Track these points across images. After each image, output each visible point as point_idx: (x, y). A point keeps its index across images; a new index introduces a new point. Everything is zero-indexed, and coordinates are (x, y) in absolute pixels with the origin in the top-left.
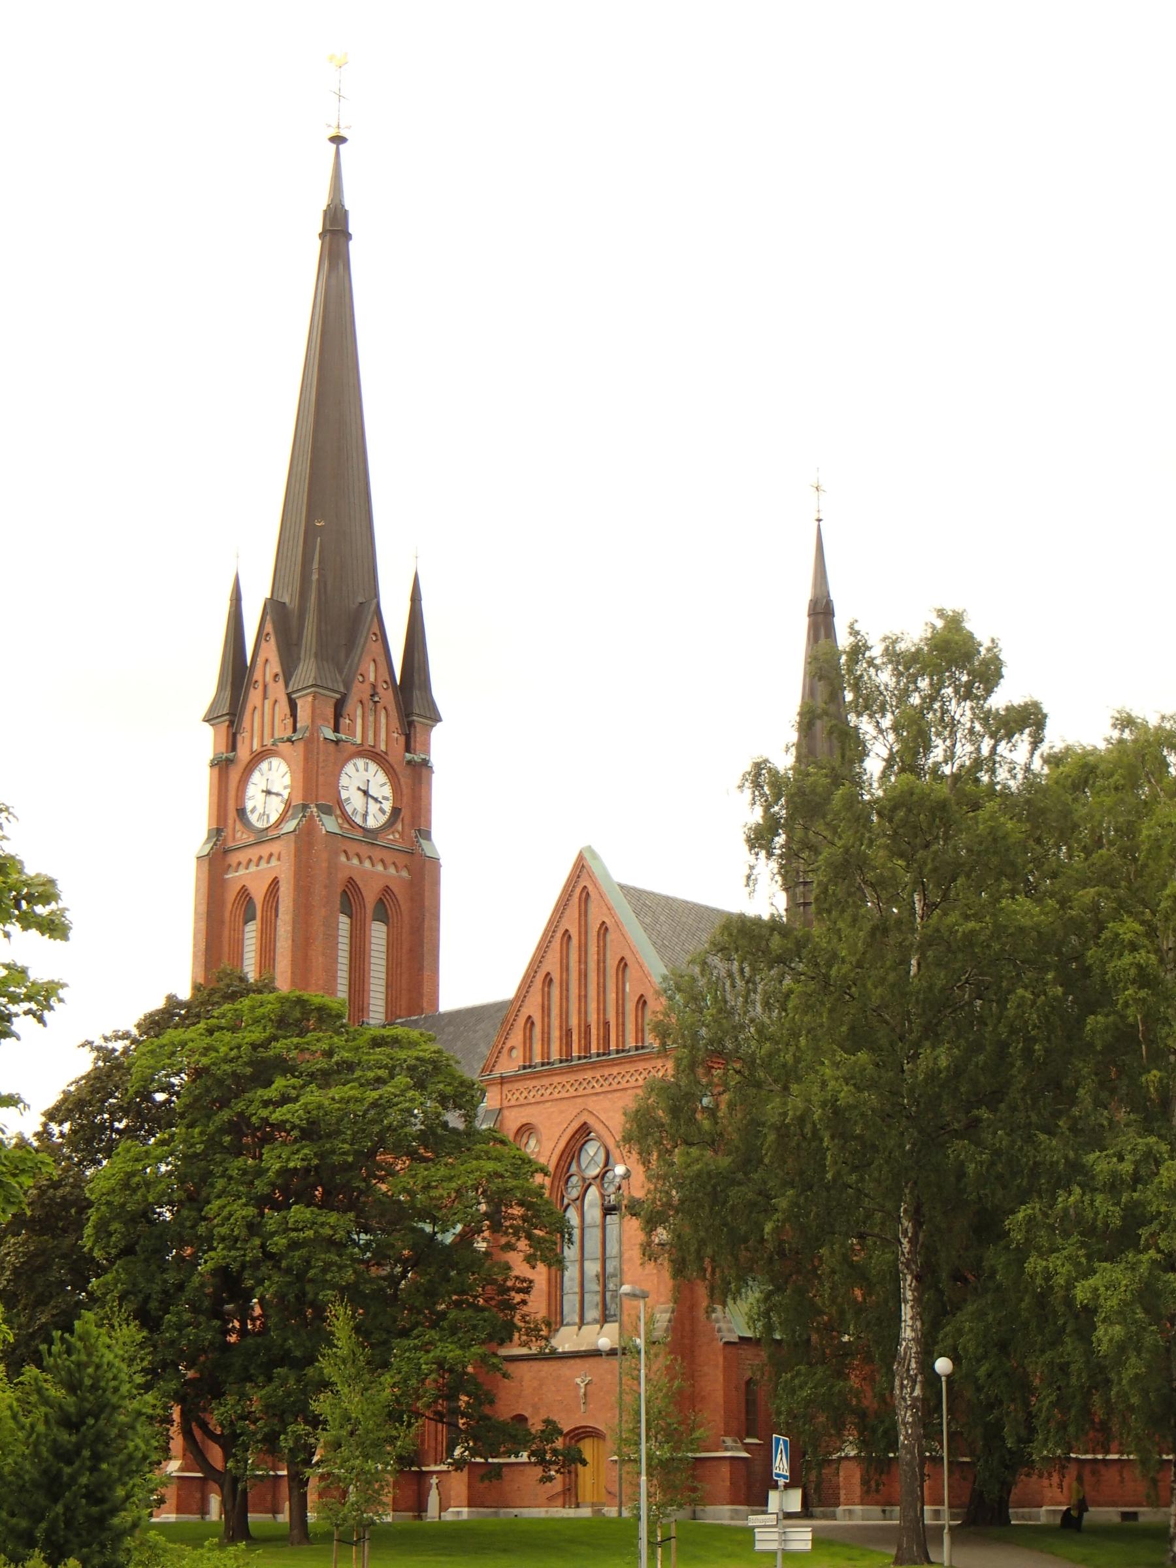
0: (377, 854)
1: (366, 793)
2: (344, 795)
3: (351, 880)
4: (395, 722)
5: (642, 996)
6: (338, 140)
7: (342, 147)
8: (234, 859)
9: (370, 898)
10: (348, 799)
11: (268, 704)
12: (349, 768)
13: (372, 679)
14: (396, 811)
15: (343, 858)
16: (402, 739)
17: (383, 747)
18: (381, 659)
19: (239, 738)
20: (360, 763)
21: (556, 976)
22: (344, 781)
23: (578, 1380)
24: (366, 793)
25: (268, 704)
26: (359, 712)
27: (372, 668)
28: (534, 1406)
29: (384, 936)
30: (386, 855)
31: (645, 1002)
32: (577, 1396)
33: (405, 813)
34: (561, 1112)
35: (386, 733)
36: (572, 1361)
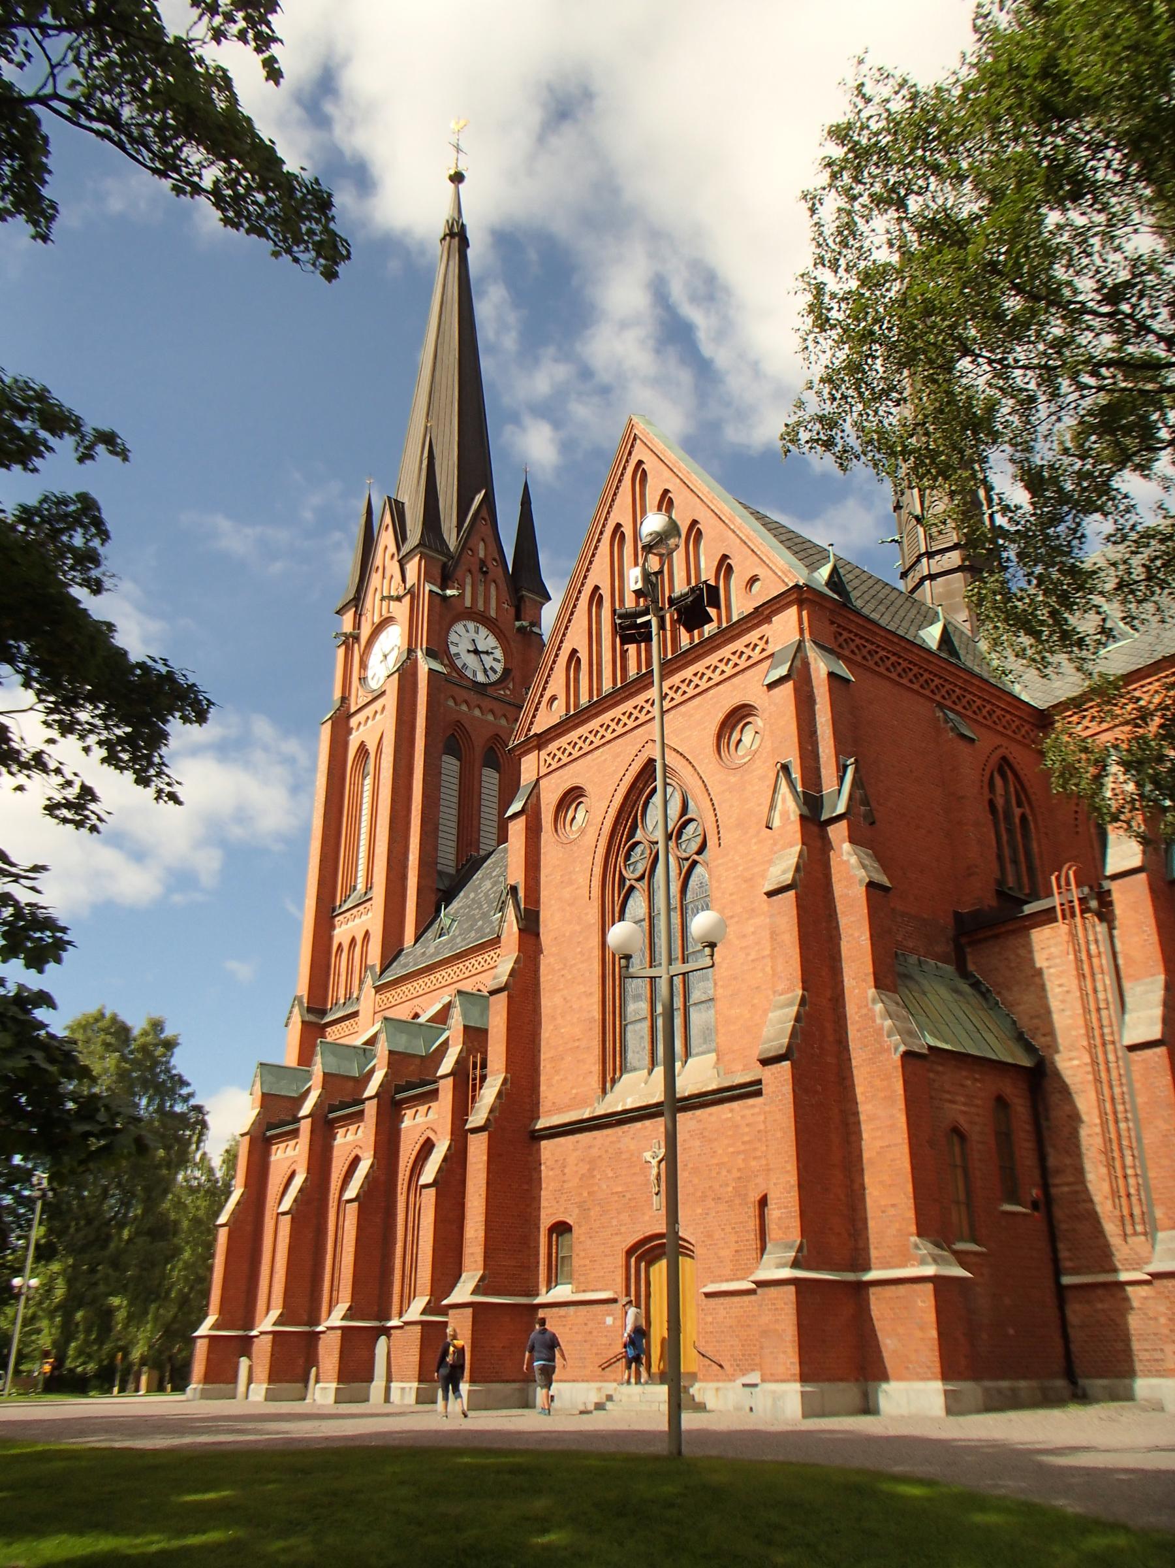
0: (487, 703)
1: (476, 652)
2: (453, 650)
3: (459, 724)
4: (505, 595)
5: (725, 557)
6: (457, 178)
7: (461, 186)
8: (353, 722)
9: (479, 741)
10: (458, 654)
11: (386, 582)
12: (459, 627)
13: (482, 554)
14: (506, 671)
15: (451, 703)
16: (512, 611)
17: (493, 614)
18: (491, 541)
19: (363, 618)
20: (471, 625)
21: (605, 592)
22: (453, 637)
23: (647, 1155)
24: (476, 652)
25: (386, 582)
26: (468, 580)
27: (482, 545)
28: (580, 1205)
29: (496, 782)
30: (496, 706)
31: (730, 568)
32: (647, 1183)
33: (516, 673)
34: (618, 755)
35: (494, 602)
36: (639, 1125)
